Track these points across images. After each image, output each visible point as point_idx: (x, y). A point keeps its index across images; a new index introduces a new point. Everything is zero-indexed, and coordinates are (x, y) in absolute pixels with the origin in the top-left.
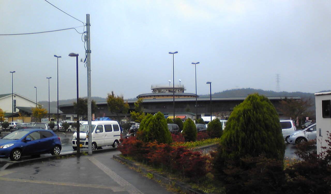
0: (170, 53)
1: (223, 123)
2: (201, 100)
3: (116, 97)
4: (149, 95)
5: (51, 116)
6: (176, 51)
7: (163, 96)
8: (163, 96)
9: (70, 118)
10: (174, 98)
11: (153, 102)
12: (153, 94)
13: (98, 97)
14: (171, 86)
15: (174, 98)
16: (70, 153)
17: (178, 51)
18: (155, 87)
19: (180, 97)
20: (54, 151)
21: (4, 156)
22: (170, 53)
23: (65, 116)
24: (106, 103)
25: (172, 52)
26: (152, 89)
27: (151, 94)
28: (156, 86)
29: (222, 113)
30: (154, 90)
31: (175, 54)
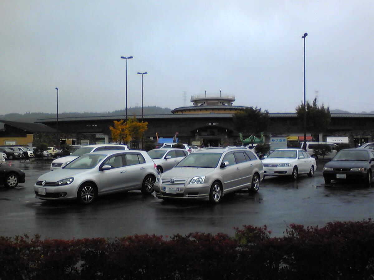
0: (122, 57)
1: (302, 147)
2: (179, 117)
3: (319, 108)
4: (187, 108)
5: (69, 136)
6: (131, 56)
7: (213, 109)
8: (213, 109)
9: (104, 139)
10: (126, 117)
11: (159, 118)
12: (194, 108)
13: (11, 114)
14: (206, 97)
15: (126, 117)
16: (234, 189)
17: (133, 56)
18: (196, 98)
19: (184, 113)
20: (9, 184)
21: (207, 194)
22: (122, 57)
23: (95, 135)
24: (296, 115)
25: (125, 57)
26: (192, 100)
27: (192, 107)
28: (198, 97)
29: (352, 133)
30: (196, 101)
31: (129, 59)
